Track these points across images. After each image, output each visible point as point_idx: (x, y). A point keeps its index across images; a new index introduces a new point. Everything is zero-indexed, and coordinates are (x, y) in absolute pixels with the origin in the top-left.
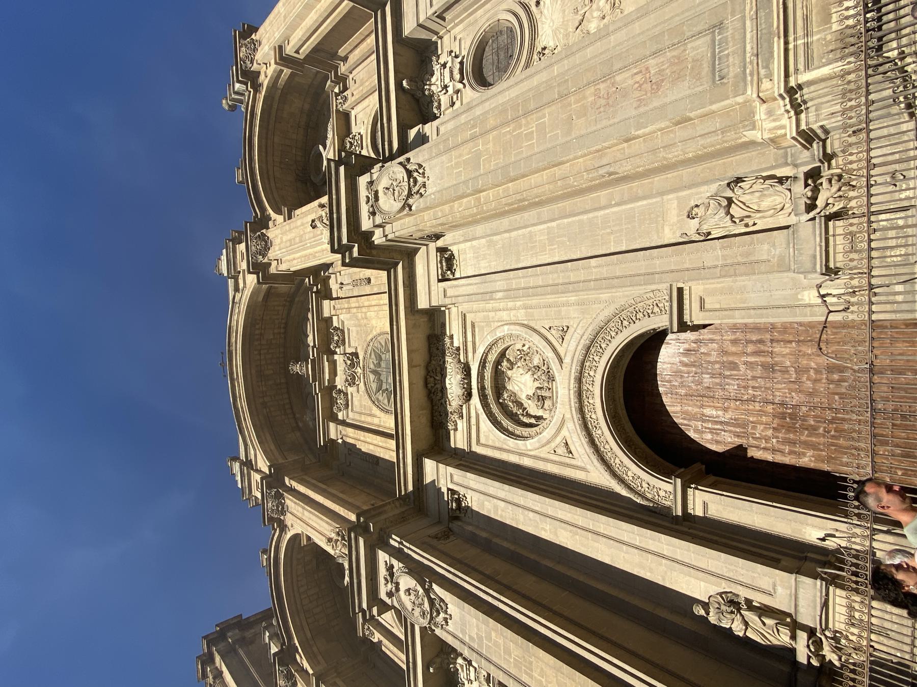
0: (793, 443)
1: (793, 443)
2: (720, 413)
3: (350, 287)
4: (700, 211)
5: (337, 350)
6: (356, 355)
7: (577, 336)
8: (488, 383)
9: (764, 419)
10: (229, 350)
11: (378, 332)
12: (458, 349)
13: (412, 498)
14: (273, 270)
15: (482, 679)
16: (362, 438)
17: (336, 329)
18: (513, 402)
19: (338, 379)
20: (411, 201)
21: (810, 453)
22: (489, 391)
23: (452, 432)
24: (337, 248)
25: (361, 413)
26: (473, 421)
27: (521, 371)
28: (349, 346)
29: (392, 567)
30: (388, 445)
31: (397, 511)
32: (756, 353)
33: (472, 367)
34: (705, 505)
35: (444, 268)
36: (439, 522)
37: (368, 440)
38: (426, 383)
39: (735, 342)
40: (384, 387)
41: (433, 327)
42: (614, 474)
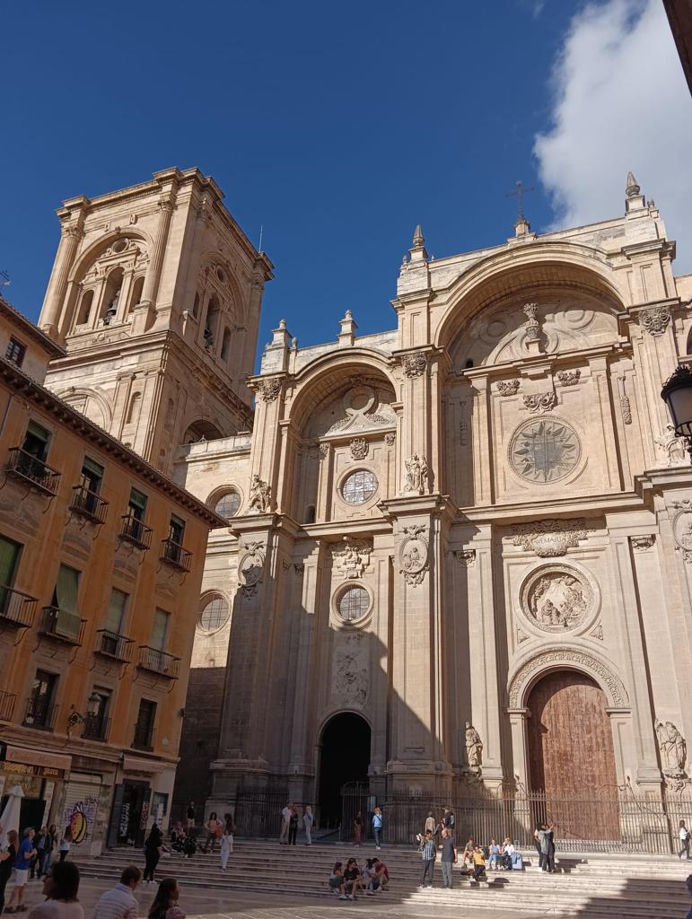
0: (553, 759)
1: (553, 757)
2: (561, 724)
3: (622, 393)
4: (670, 728)
5: (556, 378)
6: (556, 403)
7: (596, 647)
8: (553, 569)
9: (562, 746)
10: (541, 243)
11: (581, 437)
12: (577, 546)
13: (461, 520)
14: (631, 327)
15: (350, 574)
16: (481, 426)
17: (578, 374)
18: (543, 588)
19: (528, 381)
20: (681, 550)
21: (550, 767)
22: (547, 571)
23: (511, 541)
24: (648, 475)
25: (501, 417)
26: (524, 560)
27: (566, 593)
28: (562, 393)
29: (424, 531)
30: (483, 464)
31: (451, 514)
32: (597, 743)
33: (564, 558)
34: (516, 724)
35: (640, 542)
36: (449, 543)
37: (482, 436)
38: (545, 520)
39: (602, 732)
40: (531, 441)
41: (591, 519)
42: (517, 673)
